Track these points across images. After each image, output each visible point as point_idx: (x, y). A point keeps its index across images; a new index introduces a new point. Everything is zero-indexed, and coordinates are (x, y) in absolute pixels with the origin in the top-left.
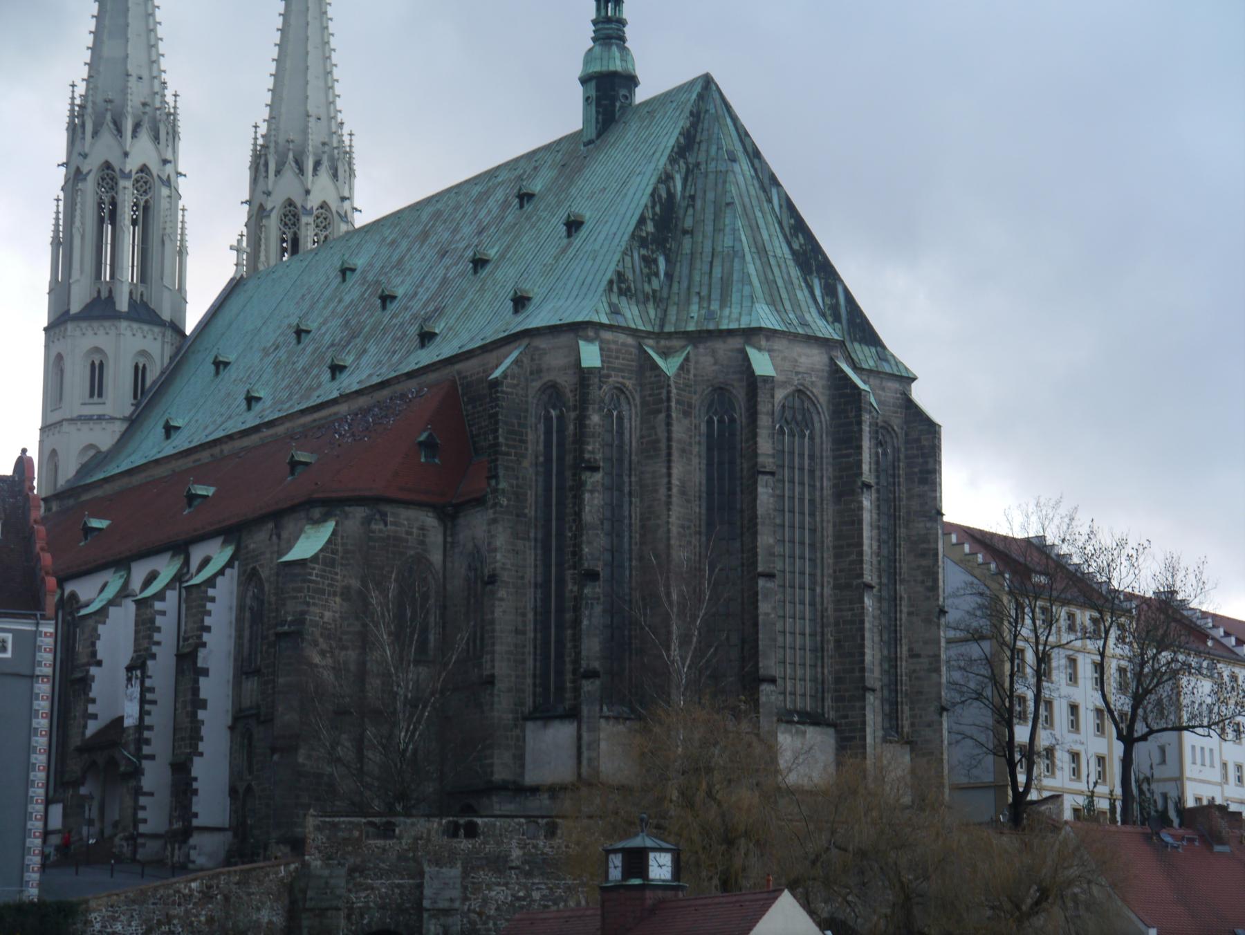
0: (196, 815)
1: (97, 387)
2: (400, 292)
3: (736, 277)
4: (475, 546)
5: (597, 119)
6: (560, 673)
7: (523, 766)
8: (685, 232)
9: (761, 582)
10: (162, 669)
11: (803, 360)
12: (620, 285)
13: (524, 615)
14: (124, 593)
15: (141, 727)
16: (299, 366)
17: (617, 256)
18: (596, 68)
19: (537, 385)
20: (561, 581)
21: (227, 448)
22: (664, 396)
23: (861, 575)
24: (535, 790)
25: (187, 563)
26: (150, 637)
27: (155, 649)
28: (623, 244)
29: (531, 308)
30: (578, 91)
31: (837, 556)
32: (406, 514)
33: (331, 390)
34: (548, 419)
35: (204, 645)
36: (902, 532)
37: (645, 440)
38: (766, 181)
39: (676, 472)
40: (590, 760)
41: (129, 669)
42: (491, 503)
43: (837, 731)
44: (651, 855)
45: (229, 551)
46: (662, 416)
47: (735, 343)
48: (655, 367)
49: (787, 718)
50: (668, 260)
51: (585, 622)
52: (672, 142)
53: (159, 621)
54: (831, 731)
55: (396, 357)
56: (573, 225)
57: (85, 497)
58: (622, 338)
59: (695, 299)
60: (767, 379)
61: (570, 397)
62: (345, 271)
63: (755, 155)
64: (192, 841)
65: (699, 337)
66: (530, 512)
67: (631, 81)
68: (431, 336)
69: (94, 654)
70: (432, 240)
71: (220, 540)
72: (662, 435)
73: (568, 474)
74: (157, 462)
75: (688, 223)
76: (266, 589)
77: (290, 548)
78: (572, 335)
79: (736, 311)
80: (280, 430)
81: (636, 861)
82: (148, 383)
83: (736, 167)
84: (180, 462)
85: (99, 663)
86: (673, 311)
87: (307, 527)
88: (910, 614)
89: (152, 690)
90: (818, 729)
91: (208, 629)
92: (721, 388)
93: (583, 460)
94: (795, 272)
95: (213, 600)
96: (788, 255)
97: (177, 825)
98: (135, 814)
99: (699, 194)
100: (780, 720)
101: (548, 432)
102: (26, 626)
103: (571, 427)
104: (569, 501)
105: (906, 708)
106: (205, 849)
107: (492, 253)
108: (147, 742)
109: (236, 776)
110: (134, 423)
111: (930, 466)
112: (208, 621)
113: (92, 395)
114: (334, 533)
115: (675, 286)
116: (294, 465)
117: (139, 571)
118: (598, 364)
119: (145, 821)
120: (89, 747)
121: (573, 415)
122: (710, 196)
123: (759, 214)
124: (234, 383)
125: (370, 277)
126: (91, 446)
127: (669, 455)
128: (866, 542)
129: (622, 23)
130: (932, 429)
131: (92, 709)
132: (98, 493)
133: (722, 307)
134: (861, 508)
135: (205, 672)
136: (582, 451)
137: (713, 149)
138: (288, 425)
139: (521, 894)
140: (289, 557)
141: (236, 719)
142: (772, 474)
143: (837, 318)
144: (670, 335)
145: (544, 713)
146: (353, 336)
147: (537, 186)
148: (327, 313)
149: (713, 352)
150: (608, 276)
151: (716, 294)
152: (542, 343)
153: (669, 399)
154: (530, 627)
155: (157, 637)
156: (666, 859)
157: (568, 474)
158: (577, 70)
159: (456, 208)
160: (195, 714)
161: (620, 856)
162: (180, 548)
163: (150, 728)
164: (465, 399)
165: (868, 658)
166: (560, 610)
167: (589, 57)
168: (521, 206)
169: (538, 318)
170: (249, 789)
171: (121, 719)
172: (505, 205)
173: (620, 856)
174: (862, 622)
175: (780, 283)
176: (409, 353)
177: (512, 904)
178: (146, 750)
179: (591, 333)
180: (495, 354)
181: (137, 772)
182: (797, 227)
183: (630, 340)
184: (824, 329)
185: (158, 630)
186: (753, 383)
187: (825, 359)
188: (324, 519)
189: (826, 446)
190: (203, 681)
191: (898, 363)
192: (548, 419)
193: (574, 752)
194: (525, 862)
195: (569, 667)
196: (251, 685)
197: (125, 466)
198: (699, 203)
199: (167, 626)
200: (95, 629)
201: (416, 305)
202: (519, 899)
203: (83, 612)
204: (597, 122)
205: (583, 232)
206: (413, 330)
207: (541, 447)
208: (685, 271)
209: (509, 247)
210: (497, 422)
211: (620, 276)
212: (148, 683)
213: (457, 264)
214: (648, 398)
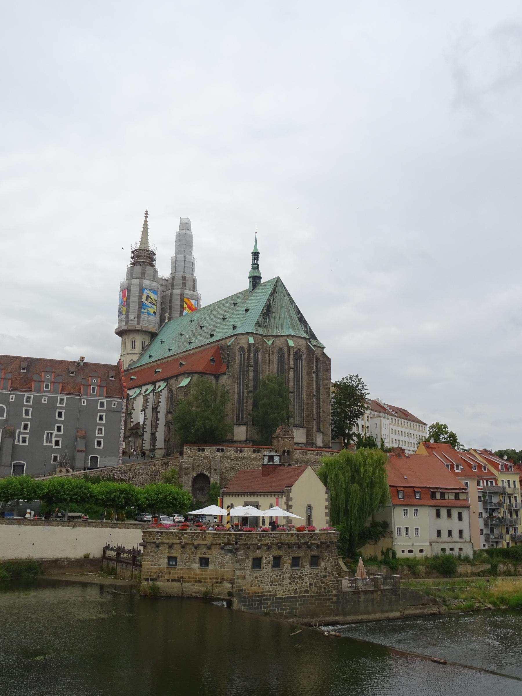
0: (156, 445)
1: (133, 346)
2: (205, 325)
3: (285, 323)
4: (223, 384)
6: (242, 414)
7: (233, 436)
8: (273, 312)
9: (290, 394)
10: (149, 411)
11: (300, 342)
12: (258, 324)
13: (234, 400)
14: (140, 393)
15: (144, 425)
16: (181, 342)
17: (258, 317)
18: (253, 275)
19: (239, 346)
20: (243, 393)
21: (164, 361)
22: (268, 349)
23: (313, 393)
24: (236, 442)
25: (155, 387)
26: (146, 404)
27: (147, 407)
28: (259, 315)
29: (237, 329)
30: (248, 280)
31: (308, 388)
32: (207, 376)
33: (189, 347)
34: (241, 355)
35: (159, 406)
36: (321, 383)
38: (292, 301)
39: (270, 367)
40: (249, 434)
41: (141, 411)
42: (227, 374)
43: (307, 429)
44: (275, 457)
45: (165, 384)
46: (268, 355)
47: (285, 338)
48: (266, 343)
49: (295, 426)
50: (269, 319)
51: (249, 402)
52: (270, 292)
53: (148, 400)
54: (305, 429)
55: (204, 340)
56: (247, 310)
57: (130, 372)
58: (259, 336)
59: (275, 328)
60: (292, 347)
61: (246, 350)
62: (192, 321)
63: (289, 295)
64: (155, 451)
65: (276, 336)
66: (236, 376)
67: (260, 278)
68: (213, 335)
69: (133, 407)
70: (213, 313)
72: (268, 359)
73: (245, 367)
74: (147, 364)
76: (174, 393)
77: (180, 384)
78: (247, 335)
79: (285, 331)
80: (177, 356)
81: (271, 458)
82: (145, 346)
83: (285, 298)
84: (153, 364)
85: (134, 410)
86: (270, 330)
87: (184, 379)
88: (323, 402)
89: (146, 416)
90: (302, 429)
91: (160, 402)
93: (249, 364)
94: (298, 322)
95: (161, 395)
96: (297, 318)
97: (152, 448)
98: (142, 445)
99: (276, 304)
100: (294, 426)
101: (241, 358)
102: (120, 400)
103: (246, 357)
104: (246, 374)
105: (322, 424)
106: (159, 453)
107: (227, 317)
108: (145, 428)
109: (166, 436)
110: (141, 355)
111: (328, 368)
112: (160, 400)
113: (132, 348)
114: (190, 380)
115: (271, 324)
116: (181, 364)
117: (144, 388)
118: (253, 342)
119: (144, 446)
120: (131, 429)
121: (247, 354)
122: (279, 304)
123: (290, 309)
124: (166, 346)
125: (198, 322)
126: (132, 360)
127: (269, 364)
128: (314, 385)
129: (258, 265)
130: (329, 359)
131: (132, 420)
132: (133, 371)
133: (282, 330)
134: (313, 377)
135: (159, 412)
136: (249, 362)
137: (280, 294)
138: (179, 355)
140: (180, 386)
141: (166, 423)
142: (293, 368)
143: (307, 333)
144: (269, 336)
145: (239, 423)
146: (194, 335)
147: (238, 302)
148: (188, 330)
149: (280, 340)
150: (255, 322)
151: (280, 326)
152: (239, 337)
153: (269, 351)
154: (236, 403)
155: (148, 404)
156: (278, 458)
157: (245, 367)
158: (248, 275)
159: (218, 306)
160: (156, 422)
161: (267, 457)
162: (154, 383)
163: (146, 425)
165: (314, 412)
166: (243, 399)
167: (250, 272)
168: (234, 306)
169: (238, 331)
170: (169, 440)
171: (139, 422)
172: (230, 306)
173: (267, 457)
174: (313, 404)
175: (295, 324)
176: (208, 339)
177: (232, 468)
178: (145, 430)
179: (251, 335)
180: (228, 339)
181: (143, 435)
182: (299, 312)
183: (260, 337)
184: (306, 336)
185: (148, 402)
186: (289, 348)
187: (305, 343)
188: (188, 377)
189: (305, 362)
190: (158, 414)
191: (321, 344)
192: (241, 355)
193: (246, 433)
194: (235, 458)
195: (245, 413)
196: (170, 416)
197: (139, 365)
198: (276, 306)
199: (150, 401)
200: (133, 402)
201: (209, 328)
202: (233, 467)
203: (130, 398)
205: (249, 312)
206: (209, 334)
208: (273, 322)
209: (231, 315)
210: (229, 355)
211: (258, 322)
212: (146, 415)
213: (219, 319)
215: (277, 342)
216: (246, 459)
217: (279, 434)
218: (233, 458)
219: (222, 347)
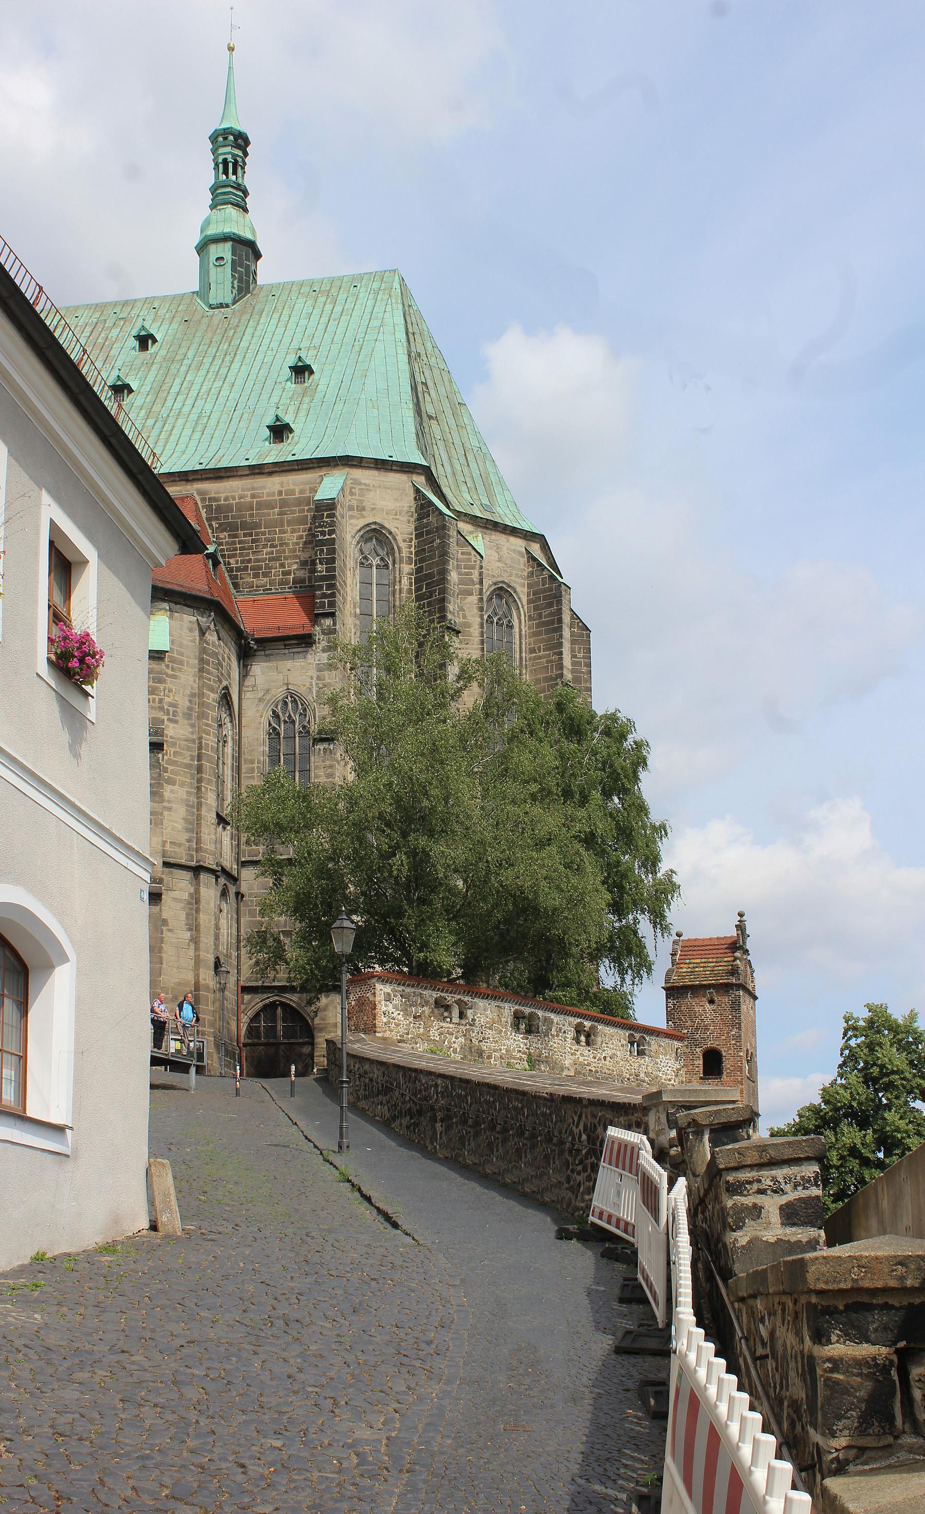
5: (233, 283)
8: (430, 417)
22: (475, 576)
47: (518, 544)
75: (431, 410)
92: (501, 589)
101: (366, 583)
103: (405, 581)
122: (441, 389)
149: (498, 548)
204: (233, 287)
207: (358, 598)
219: (218, 511)
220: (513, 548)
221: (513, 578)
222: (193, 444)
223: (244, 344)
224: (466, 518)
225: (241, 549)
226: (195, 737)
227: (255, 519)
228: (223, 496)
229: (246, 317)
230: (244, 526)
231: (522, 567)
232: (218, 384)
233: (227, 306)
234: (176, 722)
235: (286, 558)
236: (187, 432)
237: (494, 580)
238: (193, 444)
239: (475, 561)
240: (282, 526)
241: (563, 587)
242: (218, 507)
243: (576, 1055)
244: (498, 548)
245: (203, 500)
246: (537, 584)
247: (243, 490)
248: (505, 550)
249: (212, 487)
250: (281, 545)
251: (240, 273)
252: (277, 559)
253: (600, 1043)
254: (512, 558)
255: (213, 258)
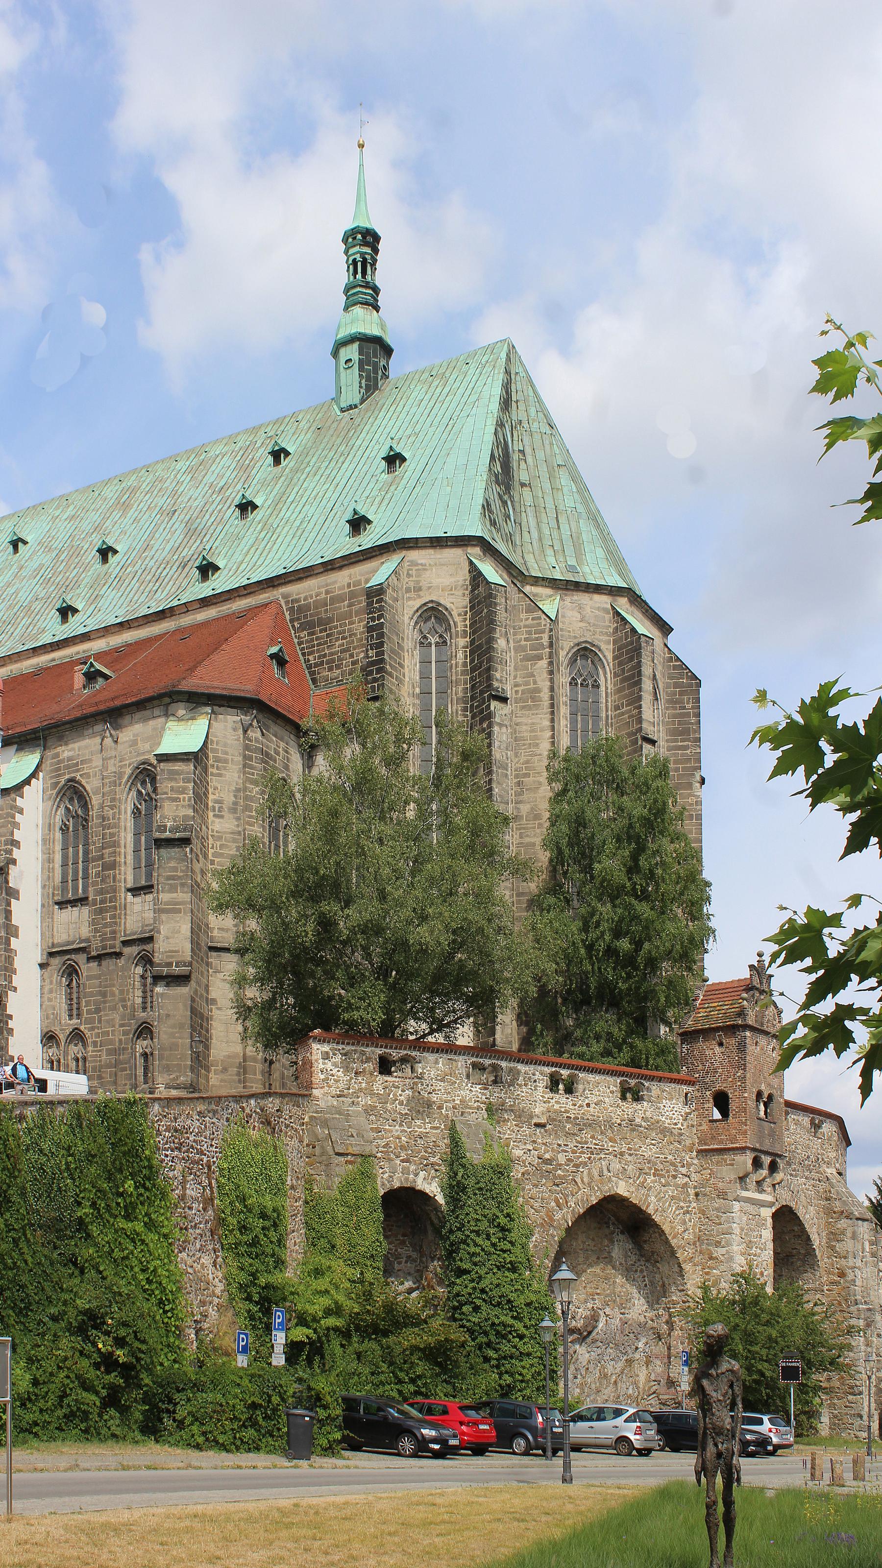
22: (545, 640)
37: (520, 689)
46: (544, 663)
47: (603, 600)
71: (15, 746)
76: (95, 801)
139: (547, 1156)
149: (580, 608)
164: (296, 625)
202: (548, 1162)
207: (418, 678)
214: (523, 643)
215: (569, 613)
216: (590, 1124)
217: (741, 1013)
218: (543, 1120)
219: (299, 611)
220: (598, 605)
221: (597, 636)
222: (290, 549)
223: (359, 442)
224: (544, 583)
225: (318, 645)
226: (240, 829)
227: (329, 615)
228: (302, 596)
229: (369, 414)
230: (321, 622)
231: (607, 623)
232: (326, 487)
233: (356, 406)
234: (222, 817)
235: (354, 649)
236: (289, 538)
237: (576, 641)
238: (290, 549)
239: (545, 625)
240: (352, 617)
241: (643, 639)
242: (299, 607)
243: (549, 1102)
244: (580, 608)
245: (287, 603)
246: (621, 638)
247: (319, 588)
248: (588, 609)
249: (294, 590)
250: (350, 636)
251: (368, 371)
252: (348, 650)
253: (581, 1091)
254: (596, 616)
255: (343, 360)
